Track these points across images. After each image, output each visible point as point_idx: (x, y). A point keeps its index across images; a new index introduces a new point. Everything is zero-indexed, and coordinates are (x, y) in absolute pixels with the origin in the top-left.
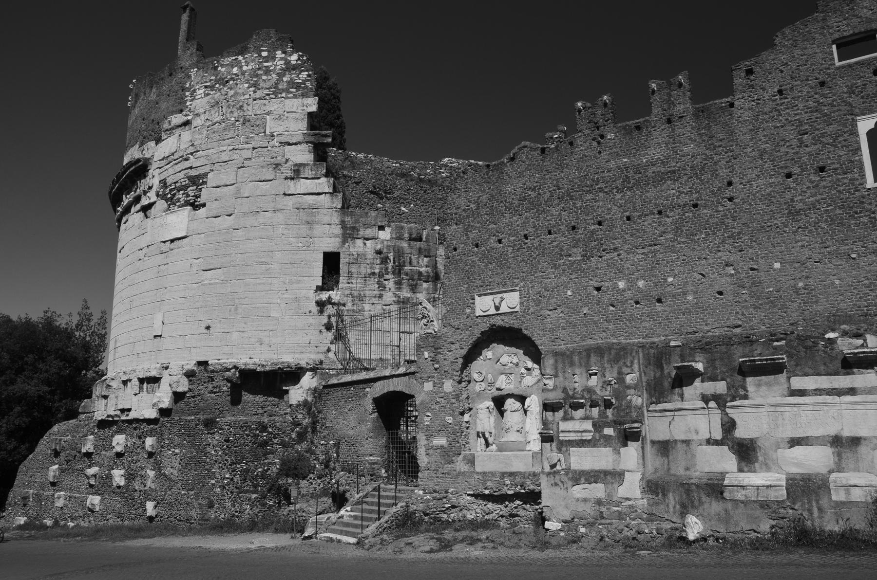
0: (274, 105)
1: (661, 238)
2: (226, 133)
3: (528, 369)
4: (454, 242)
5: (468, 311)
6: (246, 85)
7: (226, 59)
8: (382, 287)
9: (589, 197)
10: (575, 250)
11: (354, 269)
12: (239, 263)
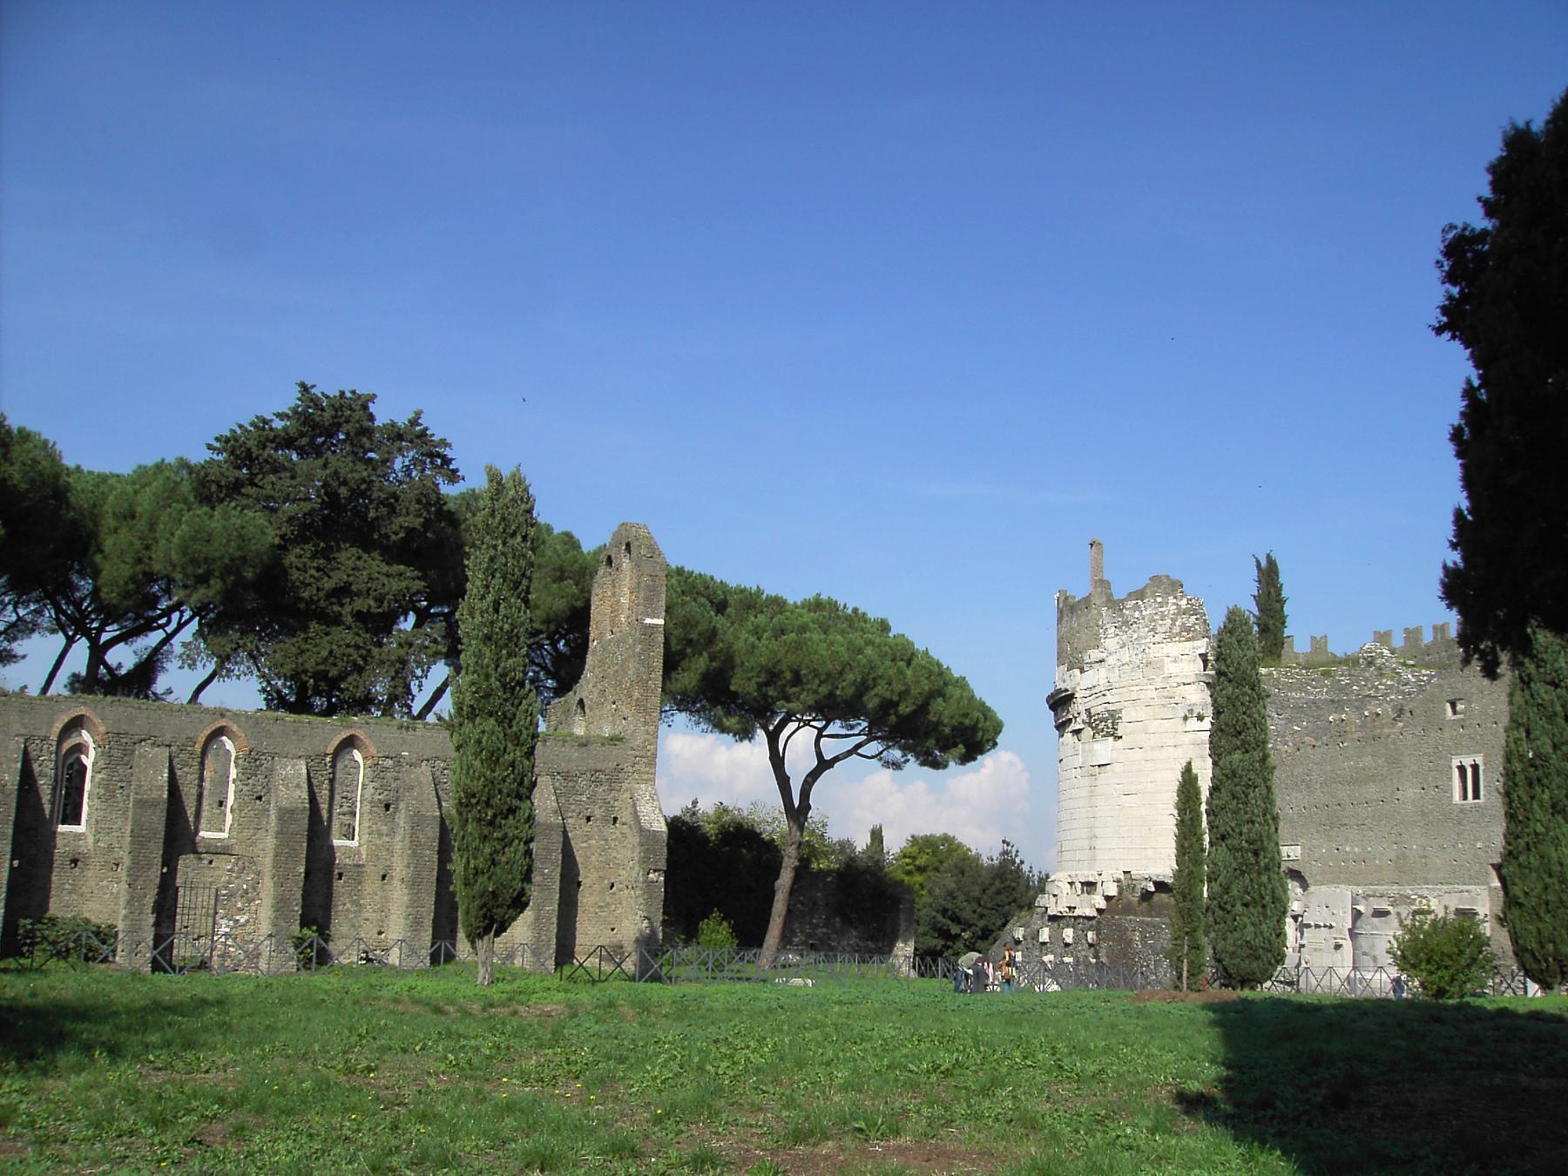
6: (1147, 629)
9: (1334, 786)
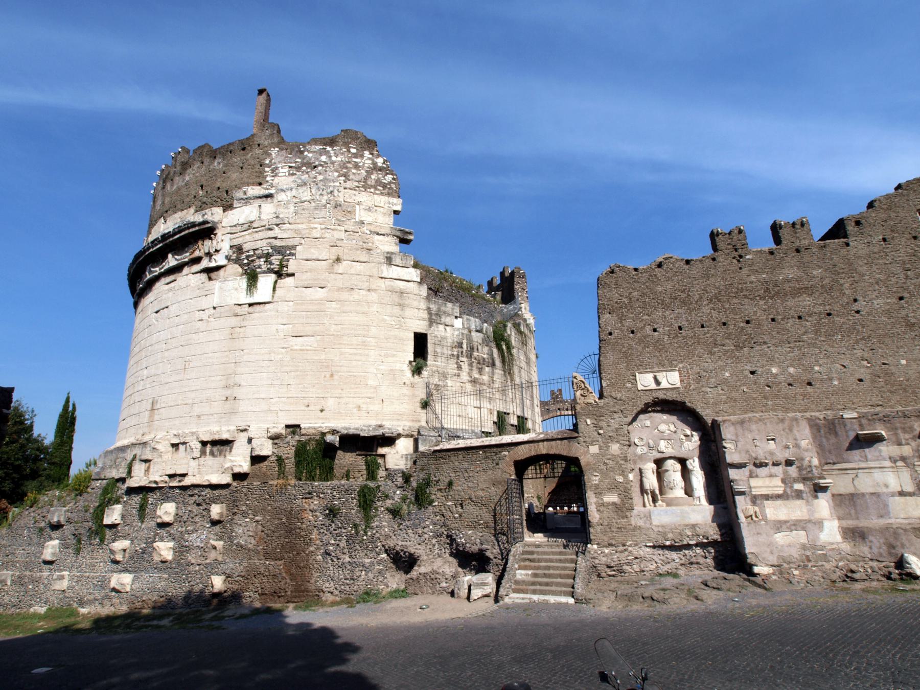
0: (364, 197)
1: (804, 336)
2: (317, 212)
3: (686, 436)
4: (609, 328)
5: (629, 385)
6: (336, 174)
7: (313, 146)
8: (459, 368)
10: (728, 341)
11: (439, 350)
12: (334, 333)
